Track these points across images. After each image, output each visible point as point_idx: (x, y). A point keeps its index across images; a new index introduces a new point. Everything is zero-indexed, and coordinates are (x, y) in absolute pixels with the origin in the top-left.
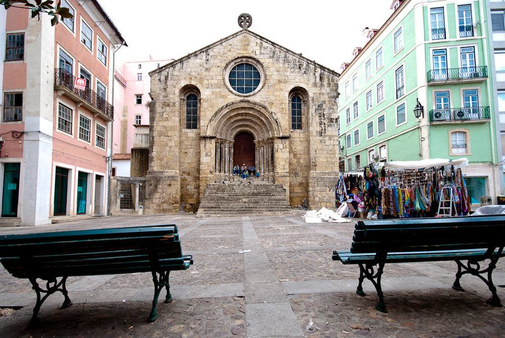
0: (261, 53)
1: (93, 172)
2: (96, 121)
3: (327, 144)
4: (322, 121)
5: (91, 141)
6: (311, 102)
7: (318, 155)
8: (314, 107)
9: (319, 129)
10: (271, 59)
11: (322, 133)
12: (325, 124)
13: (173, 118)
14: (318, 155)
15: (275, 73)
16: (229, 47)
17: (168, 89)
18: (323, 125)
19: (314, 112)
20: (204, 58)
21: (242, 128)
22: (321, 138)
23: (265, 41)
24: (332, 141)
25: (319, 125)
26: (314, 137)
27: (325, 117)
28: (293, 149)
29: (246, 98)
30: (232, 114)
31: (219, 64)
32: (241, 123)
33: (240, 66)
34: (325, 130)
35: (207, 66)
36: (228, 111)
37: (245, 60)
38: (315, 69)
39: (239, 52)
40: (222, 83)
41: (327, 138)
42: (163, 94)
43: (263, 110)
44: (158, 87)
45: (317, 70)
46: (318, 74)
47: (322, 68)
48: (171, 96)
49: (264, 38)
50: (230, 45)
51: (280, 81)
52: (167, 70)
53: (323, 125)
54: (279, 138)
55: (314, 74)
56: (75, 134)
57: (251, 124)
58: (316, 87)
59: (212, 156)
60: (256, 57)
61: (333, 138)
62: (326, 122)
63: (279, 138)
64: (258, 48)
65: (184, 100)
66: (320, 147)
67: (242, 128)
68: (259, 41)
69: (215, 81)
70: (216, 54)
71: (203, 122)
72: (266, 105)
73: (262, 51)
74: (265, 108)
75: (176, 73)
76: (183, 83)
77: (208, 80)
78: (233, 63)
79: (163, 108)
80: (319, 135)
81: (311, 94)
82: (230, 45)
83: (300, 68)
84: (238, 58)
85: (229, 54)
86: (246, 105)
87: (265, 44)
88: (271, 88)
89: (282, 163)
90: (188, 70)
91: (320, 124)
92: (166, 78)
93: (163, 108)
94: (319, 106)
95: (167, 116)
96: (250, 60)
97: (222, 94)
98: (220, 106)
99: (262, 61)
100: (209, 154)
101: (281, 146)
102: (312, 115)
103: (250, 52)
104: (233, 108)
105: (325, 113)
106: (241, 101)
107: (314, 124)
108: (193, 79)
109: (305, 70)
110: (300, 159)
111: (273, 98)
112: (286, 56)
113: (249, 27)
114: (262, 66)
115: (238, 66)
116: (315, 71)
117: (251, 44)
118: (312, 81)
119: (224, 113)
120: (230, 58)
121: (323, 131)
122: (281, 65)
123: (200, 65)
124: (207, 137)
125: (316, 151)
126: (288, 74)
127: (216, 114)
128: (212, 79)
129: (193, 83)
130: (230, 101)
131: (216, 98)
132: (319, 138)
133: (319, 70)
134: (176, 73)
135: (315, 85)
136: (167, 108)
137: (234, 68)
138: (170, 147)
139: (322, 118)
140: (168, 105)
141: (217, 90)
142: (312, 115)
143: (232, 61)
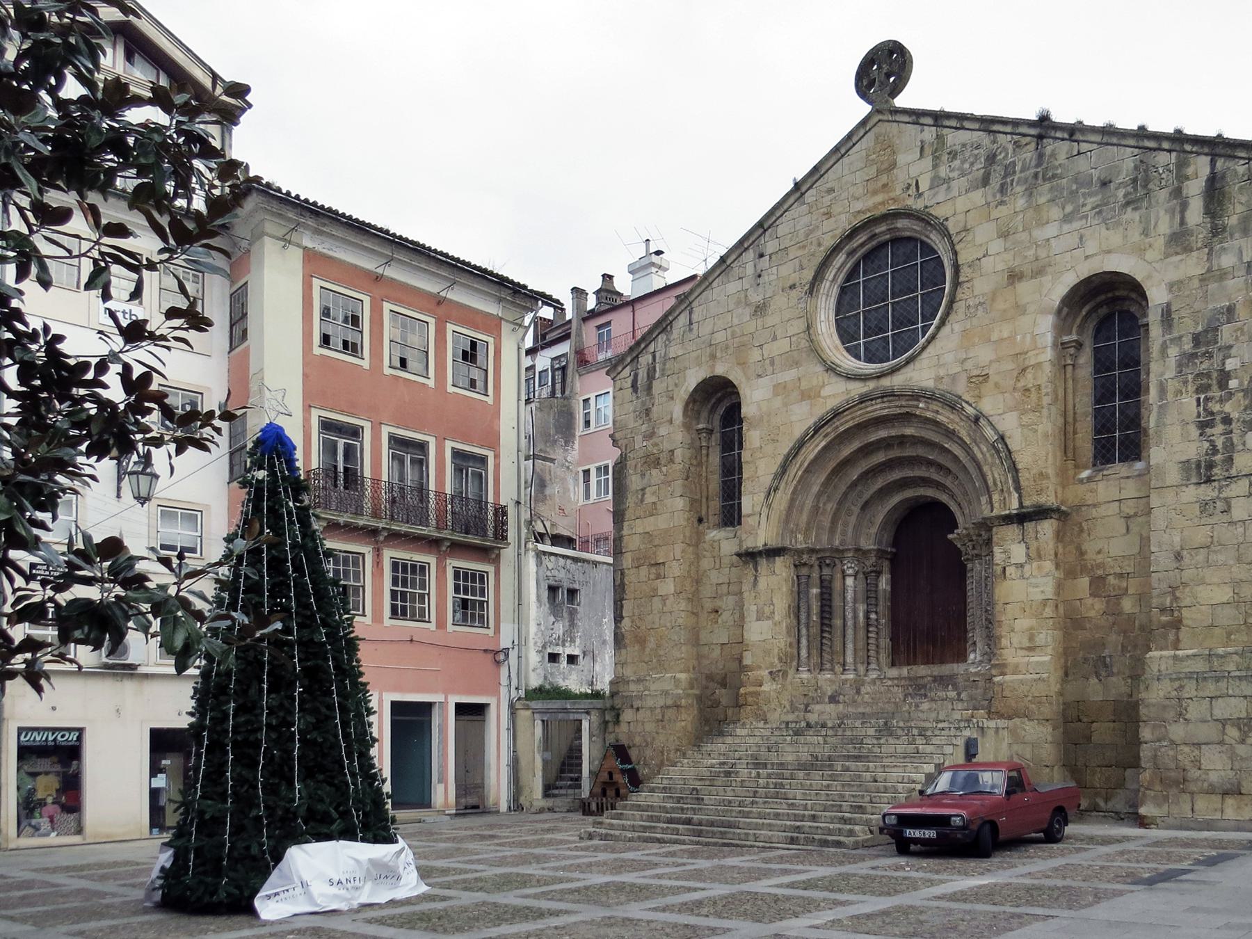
0: (937, 182)
1: (445, 702)
2: (448, 561)
4: (1216, 408)
5: (433, 618)
6: (1155, 332)
7: (1188, 574)
8: (1173, 352)
9: (1194, 449)
10: (980, 192)
11: (1210, 466)
12: (1227, 420)
13: (668, 502)
14: (1188, 574)
15: (996, 246)
16: (827, 200)
17: (655, 409)
18: (1219, 428)
19: (1170, 373)
20: (750, 270)
21: (909, 493)
22: (1207, 492)
23: (954, 123)
25: (1194, 432)
26: (1170, 496)
27: (1233, 384)
28: (1091, 556)
29: (886, 382)
30: (846, 451)
31: (794, 278)
32: (896, 475)
33: (872, 256)
34: (1230, 447)
35: (756, 298)
36: (823, 443)
37: (883, 228)
39: (859, 206)
40: (804, 344)
42: (644, 428)
43: (945, 417)
44: (632, 405)
45: (1190, 171)
46: (1195, 188)
47: (1217, 147)
48: (663, 431)
49: (949, 116)
50: (831, 190)
51: (1014, 277)
52: (651, 348)
53: (1219, 428)
54: (1008, 519)
55: (1177, 193)
56: (374, 611)
57: (935, 476)
58: (1188, 249)
60: (919, 205)
63: (1008, 519)
64: (928, 162)
65: (710, 432)
66: (1201, 536)
67: (909, 493)
68: (929, 134)
69: (782, 345)
70: (787, 243)
71: (749, 502)
72: (961, 388)
73: (943, 171)
74: (952, 404)
75: (674, 350)
76: (693, 379)
77: (761, 346)
78: (841, 258)
79: (643, 475)
80: (1194, 480)
81: (1157, 295)
82: (831, 190)
84: (854, 232)
85: (828, 225)
86: (878, 409)
87: (955, 138)
88: (980, 312)
89: (1023, 623)
90: (706, 329)
91: (1203, 426)
92: (651, 376)
93: (643, 475)
94: (1197, 339)
95: (654, 499)
96: (901, 223)
97: (804, 385)
98: (798, 432)
99: (939, 212)
100: (767, 610)
101: (1018, 552)
102: (1162, 391)
103: (898, 192)
104: (842, 429)
105: (1230, 364)
106: (864, 399)
107: (1173, 432)
108: (718, 355)
109: (1130, 189)
110: (1119, 597)
111: (983, 355)
112: (1041, 156)
113: (896, 90)
114: (946, 233)
115: (866, 257)
116: (1182, 178)
117: (902, 159)
119: (811, 456)
120: (829, 242)
121: (1219, 457)
122: (1021, 203)
123: (738, 303)
124: (760, 553)
125: (1178, 557)
126: (1051, 230)
127: (784, 469)
128: (775, 339)
129: (720, 370)
130: (831, 404)
131: (786, 405)
132: (1192, 493)
133: (1201, 166)
134: (674, 350)
135: (1179, 241)
136: (655, 472)
138: (664, 599)
139: (1216, 393)
140: (657, 463)
141: (789, 375)
142: (1162, 391)
143: (836, 250)
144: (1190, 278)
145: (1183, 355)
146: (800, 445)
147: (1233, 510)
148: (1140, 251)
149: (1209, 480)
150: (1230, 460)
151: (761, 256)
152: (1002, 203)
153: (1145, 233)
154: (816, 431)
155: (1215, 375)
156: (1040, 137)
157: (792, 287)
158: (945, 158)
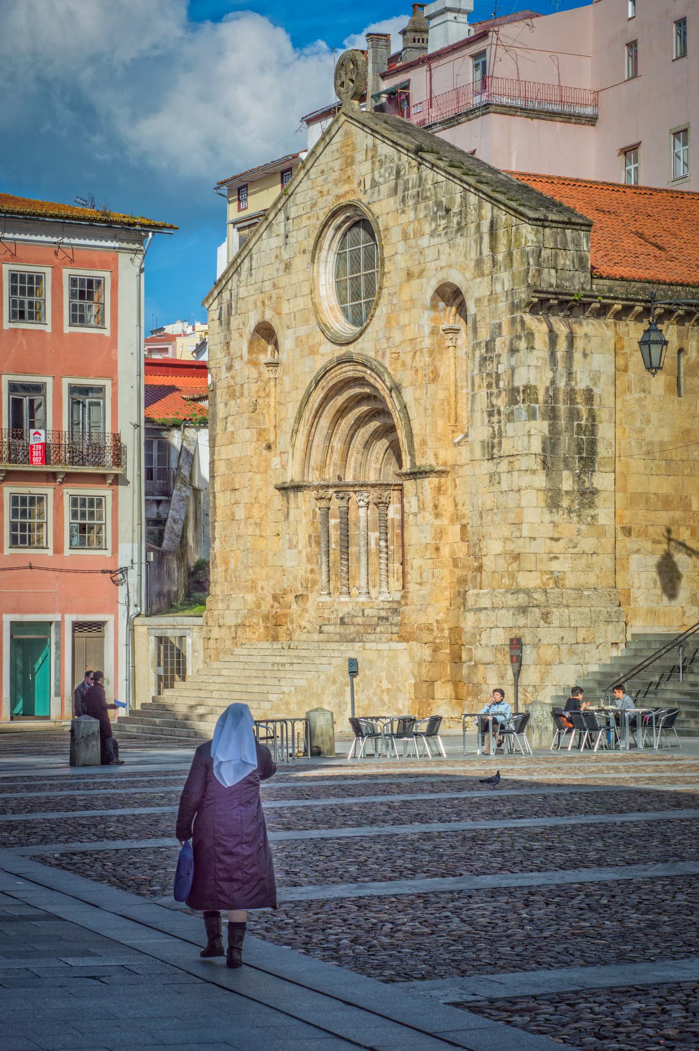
3: (504, 486)
11: (493, 447)
24: (515, 474)
25: (486, 419)
27: (501, 384)
38: (480, 207)
41: (504, 466)
55: (478, 226)
59: (300, 547)
61: (517, 465)
62: (501, 402)
78: (330, 232)
80: (486, 457)
83: (448, 211)
91: (490, 414)
112: (420, 178)
118: (473, 255)
119: (316, 406)
121: (496, 441)
128: (296, 296)
136: (232, 402)
139: (495, 390)
143: (325, 225)
144: (484, 297)
145: (481, 356)
146: (308, 395)
147: (502, 482)
148: (464, 269)
149: (492, 458)
150: (500, 443)
151: (288, 219)
152: (403, 212)
153: (465, 256)
154: (317, 384)
155: (494, 375)
156: (420, 164)
157: (304, 252)
158: (377, 164)
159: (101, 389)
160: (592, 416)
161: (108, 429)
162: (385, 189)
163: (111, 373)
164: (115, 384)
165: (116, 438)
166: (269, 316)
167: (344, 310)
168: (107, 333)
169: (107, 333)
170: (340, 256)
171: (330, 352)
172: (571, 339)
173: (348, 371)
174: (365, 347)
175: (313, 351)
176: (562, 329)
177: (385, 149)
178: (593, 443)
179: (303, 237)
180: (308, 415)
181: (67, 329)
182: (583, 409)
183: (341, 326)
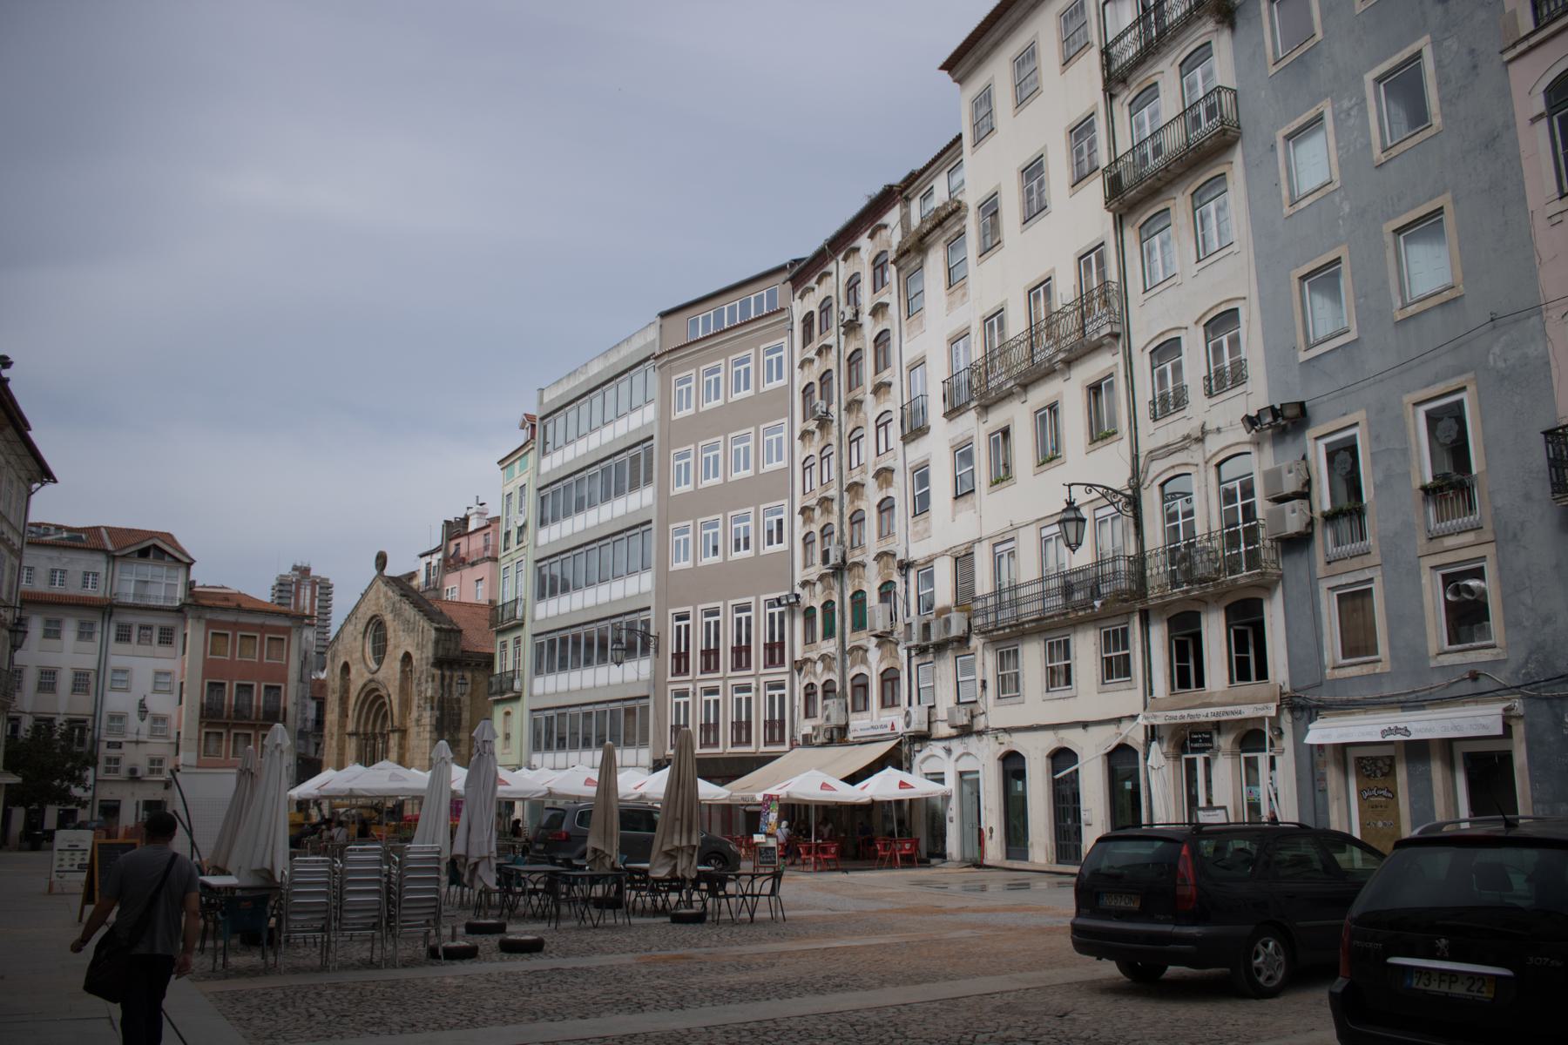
62: (422, 702)
78: (371, 626)
137: (375, 631)
148: (412, 646)
159: (279, 688)
160: (460, 708)
161: (282, 705)
162: (389, 609)
163: (285, 680)
164: (286, 685)
165: (285, 709)
166: (348, 659)
167: (375, 659)
168: (284, 662)
169: (284, 662)
170: (374, 636)
171: (368, 676)
172: (451, 678)
173: (373, 685)
174: (380, 676)
175: (362, 676)
176: (447, 673)
177: (390, 593)
178: (460, 720)
179: (361, 627)
180: (359, 704)
181: (265, 661)
182: (456, 706)
183: (374, 666)
